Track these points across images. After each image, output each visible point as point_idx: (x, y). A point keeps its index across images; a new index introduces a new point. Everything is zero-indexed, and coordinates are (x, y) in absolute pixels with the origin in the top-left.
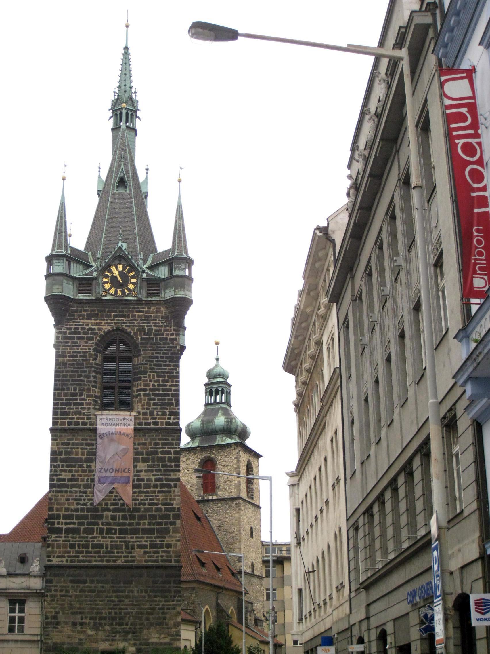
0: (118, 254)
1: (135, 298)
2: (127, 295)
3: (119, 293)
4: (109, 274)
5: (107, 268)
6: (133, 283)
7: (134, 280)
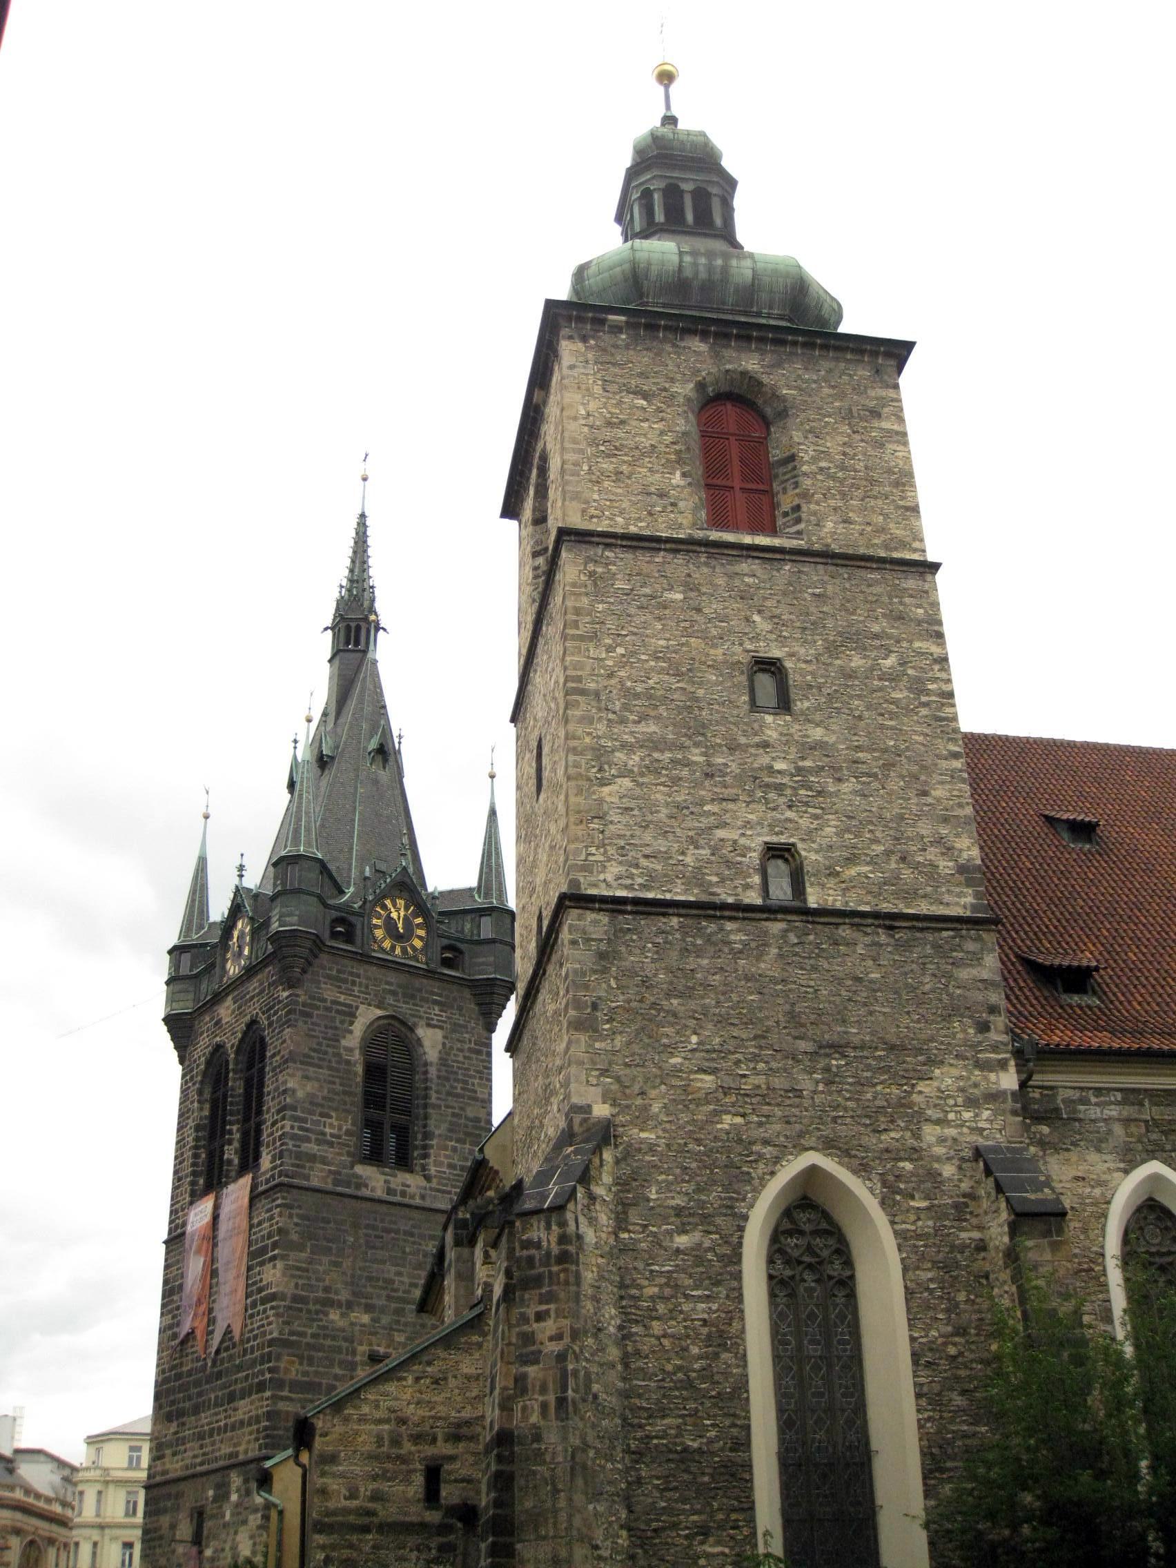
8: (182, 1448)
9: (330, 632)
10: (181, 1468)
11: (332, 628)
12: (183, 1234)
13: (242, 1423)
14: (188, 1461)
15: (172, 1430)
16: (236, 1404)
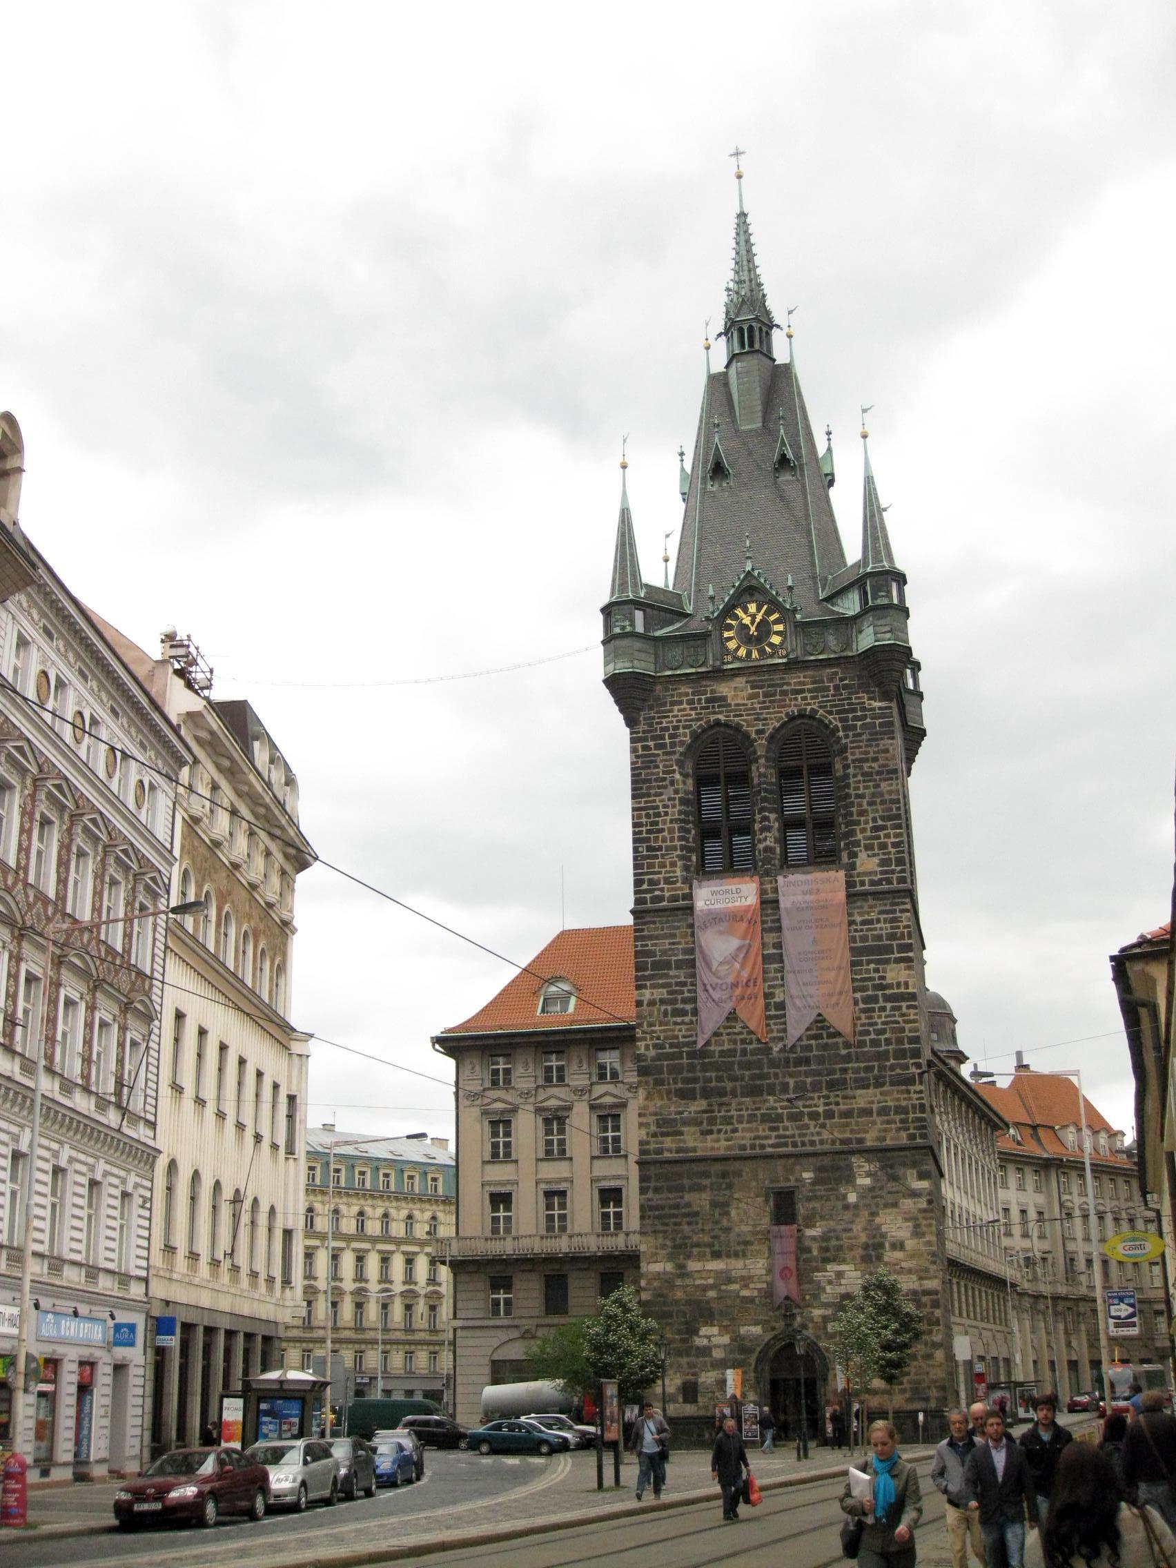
0: (746, 584)
1: (785, 660)
2: (772, 656)
3: (755, 654)
5: (728, 611)
6: (778, 633)
7: (780, 627)
8: (729, 1128)
9: (723, 337)
10: (728, 1148)
11: (726, 333)
12: (690, 909)
13: (867, 1112)
14: (748, 1143)
15: (693, 1109)
16: (849, 1092)
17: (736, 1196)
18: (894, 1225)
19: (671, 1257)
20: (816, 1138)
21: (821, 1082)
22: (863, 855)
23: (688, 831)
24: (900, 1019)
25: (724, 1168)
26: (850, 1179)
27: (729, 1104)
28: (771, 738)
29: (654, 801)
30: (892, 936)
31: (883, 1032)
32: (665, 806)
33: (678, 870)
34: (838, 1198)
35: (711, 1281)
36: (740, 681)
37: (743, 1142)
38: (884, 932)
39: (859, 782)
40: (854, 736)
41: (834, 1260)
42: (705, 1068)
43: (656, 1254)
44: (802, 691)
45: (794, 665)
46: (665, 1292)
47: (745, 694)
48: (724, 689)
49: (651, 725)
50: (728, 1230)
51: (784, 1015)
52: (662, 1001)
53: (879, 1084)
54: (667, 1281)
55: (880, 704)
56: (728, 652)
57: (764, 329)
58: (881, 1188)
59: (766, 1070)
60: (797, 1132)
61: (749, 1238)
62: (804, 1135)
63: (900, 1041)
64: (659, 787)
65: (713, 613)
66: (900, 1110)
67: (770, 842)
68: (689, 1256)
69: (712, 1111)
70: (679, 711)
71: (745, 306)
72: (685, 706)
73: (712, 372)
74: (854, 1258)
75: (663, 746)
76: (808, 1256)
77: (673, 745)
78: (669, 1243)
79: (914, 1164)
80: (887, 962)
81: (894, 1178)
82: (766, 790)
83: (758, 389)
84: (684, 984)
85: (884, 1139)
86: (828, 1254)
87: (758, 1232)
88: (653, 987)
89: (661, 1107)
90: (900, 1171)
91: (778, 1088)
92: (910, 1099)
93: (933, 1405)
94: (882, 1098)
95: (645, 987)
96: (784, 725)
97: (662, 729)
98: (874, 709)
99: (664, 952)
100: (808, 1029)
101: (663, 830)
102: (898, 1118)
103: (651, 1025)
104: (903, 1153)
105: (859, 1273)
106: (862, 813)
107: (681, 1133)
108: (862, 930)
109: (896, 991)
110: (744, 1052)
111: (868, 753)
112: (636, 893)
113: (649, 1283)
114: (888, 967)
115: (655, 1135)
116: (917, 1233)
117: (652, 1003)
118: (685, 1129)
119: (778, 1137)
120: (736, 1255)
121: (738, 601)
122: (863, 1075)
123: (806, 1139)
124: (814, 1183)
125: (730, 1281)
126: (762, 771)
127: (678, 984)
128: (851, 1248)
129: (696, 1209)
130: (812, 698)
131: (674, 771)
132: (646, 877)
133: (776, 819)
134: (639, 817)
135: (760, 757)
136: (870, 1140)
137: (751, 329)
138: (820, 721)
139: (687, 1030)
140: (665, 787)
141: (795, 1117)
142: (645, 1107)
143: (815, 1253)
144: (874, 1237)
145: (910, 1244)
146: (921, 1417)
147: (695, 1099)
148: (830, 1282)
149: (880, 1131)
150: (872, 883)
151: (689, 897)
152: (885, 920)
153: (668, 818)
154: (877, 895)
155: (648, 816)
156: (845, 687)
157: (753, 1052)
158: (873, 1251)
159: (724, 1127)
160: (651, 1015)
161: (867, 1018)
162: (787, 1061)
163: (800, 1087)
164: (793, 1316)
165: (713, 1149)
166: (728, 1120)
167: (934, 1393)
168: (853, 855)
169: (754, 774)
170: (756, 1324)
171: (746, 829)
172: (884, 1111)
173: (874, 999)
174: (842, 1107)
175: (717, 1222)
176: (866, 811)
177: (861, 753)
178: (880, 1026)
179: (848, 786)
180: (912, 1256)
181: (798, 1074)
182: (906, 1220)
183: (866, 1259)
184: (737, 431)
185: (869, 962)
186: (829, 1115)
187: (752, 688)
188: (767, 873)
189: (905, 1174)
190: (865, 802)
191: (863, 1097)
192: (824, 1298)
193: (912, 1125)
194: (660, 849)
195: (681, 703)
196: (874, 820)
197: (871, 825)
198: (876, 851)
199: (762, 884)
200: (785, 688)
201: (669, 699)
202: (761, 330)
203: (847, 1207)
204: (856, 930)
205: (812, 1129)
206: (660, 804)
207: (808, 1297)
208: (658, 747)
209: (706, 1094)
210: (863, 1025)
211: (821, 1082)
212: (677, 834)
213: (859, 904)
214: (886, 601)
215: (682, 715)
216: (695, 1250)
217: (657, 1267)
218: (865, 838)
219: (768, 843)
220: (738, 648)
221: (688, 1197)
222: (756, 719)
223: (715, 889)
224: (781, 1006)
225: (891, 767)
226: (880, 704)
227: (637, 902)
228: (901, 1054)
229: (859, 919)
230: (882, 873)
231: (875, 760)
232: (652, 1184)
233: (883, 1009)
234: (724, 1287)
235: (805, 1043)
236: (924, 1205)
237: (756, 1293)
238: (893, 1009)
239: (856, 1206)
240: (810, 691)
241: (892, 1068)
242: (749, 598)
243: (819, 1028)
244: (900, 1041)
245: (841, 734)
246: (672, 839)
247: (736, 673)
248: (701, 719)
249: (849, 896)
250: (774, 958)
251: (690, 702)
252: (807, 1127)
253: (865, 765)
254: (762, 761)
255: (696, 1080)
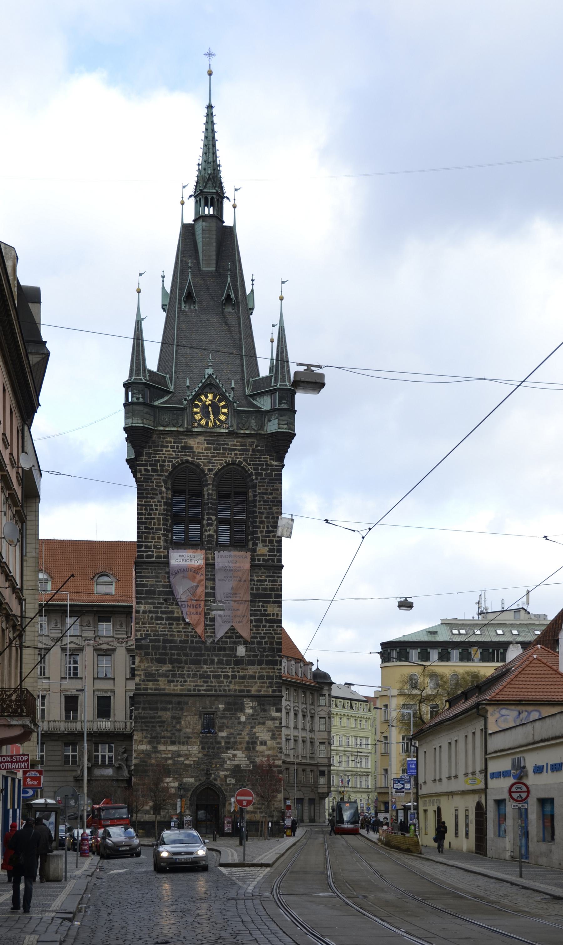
0: (208, 382)
1: (227, 431)
2: (219, 427)
4: (199, 403)
5: (197, 397)
6: (224, 414)
7: (225, 410)
8: (183, 680)
10: (181, 690)
12: (168, 563)
13: (253, 677)
14: (192, 688)
15: (164, 669)
16: (245, 667)
17: (184, 714)
18: (262, 733)
19: (150, 743)
20: (227, 688)
21: (231, 660)
22: (260, 545)
23: (167, 520)
24: (273, 632)
25: (179, 701)
26: (242, 710)
27: (183, 668)
28: (215, 475)
29: (150, 502)
30: (272, 590)
31: (264, 638)
32: (156, 505)
33: (162, 542)
34: (236, 719)
35: (170, 756)
36: (201, 439)
37: (189, 687)
38: (268, 587)
39: (261, 505)
40: (261, 479)
41: (232, 749)
42: (171, 648)
43: (142, 741)
44: (235, 450)
45: (231, 434)
46: (146, 760)
47: (203, 447)
48: (192, 442)
49: (150, 457)
50: (180, 731)
51: (214, 625)
52: (150, 612)
53: (260, 663)
54: (147, 754)
55: (276, 463)
56: (195, 421)
57: (220, 200)
58: (257, 715)
59: (203, 652)
60: (217, 684)
61: (190, 735)
62: (221, 686)
63: (272, 643)
64: (153, 494)
65: (188, 396)
66: (269, 677)
67: (211, 532)
68: (159, 743)
69: (175, 671)
70: (166, 451)
71: (210, 182)
72: (169, 449)
73: (186, 222)
74: (242, 748)
75: (156, 471)
76: (219, 745)
77: (162, 471)
78: (149, 736)
79: (274, 705)
80: (268, 602)
81: (264, 710)
82: (212, 503)
83: (214, 244)
84: (162, 604)
85: (261, 691)
86: (229, 745)
87: (195, 733)
88: (146, 603)
89: (148, 667)
90: (267, 707)
91: (209, 661)
92: (274, 672)
93: (275, 819)
94: (261, 671)
95: (141, 603)
96: (222, 468)
97: (156, 461)
98: (272, 466)
99: (152, 586)
100: (226, 633)
101: (154, 519)
102: (268, 681)
103: (143, 623)
104: (270, 699)
105: (244, 755)
106: (262, 522)
107: (158, 681)
108: (257, 585)
109: (272, 618)
110: (192, 642)
111: (267, 490)
112: (138, 552)
113: (138, 755)
114: (269, 605)
115: (144, 681)
116: (273, 738)
117: (145, 612)
118: (160, 679)
119: (207, 686)
120: (183, 743)
121: (203, 391)
122: (252, 658)
123: (222, 688)
124: (225, 710)
125: (179, 756)
126: (209, 492)
127: (159, 603)
128: (240, 743)
129: (163, 719)
130: (240, 455)
131: (161, 486)
132: (144, 544)
133: (216, 520)
134: (141, 509)
135: (209, 484)
136: (253, 690)
137: (212, 199)
138: (243, 467)
139: (163, 628)
140: (156, 494)
141: (217, 677)
142: (140, 666)
143: (223, 744)
144: (252, 738)
145: (269, 743)
146: (270, 825)
147: (165, 664)
148: (229, 759)
149: (259, 687)
150: (264, 560)
151: (167, 557)
152: (269, 580)
153: (157, 512)
154: (266, 567)
155: (146, 509)
156: (258, 451)
157: (197, 642)
158: (251, 746)
159: (180, 680)
160: (144, 619)
161: (256, 630)
162: (214, 648)
163: (220, 662)
164: (210, 774)
165: (174, 690)
166: (182, 676)
167: (276, 814)
168: (255, 544)
169: (205, 493)
170: (192, 777)
171: (199, 521)
172: (261, 677)
173: (260, 621)
174: (240, 674)
175: (175, 727)
176: (264, 521)
177: (264, 489)
178: (262, 635)
179: (255, 506)
180: (269, 749)
181: (220, 655)
182: (268, 731)
183: (248, 749)
184: (200, 270)
185: (259, 601)
186: (234, 677)
187: (208, 444)
188: (209, 549)
189: (269, 709)
190: (264, 516)
191: (252, 670)
192: (226, 766)
193: (275, 686)
194: (152, 529)
195: (167, 447)
196: (268, 527)
197: (266, 529)
198: (267, 544)
199: (206, 554)
200: (226, 446)
201: (160, 444)
202: (218, 200)
203: (240, 723)
204: (254, 584)
205: (225, 684)
206: (153, 504)
207: (218, 766)
208: (153, 471)
209: (171, 662)
210: (254, 633)
211: (231, 660)
212: (162, 522)
213: (256, 571)
214: (286, 406)
215: (167, 454)
216: (162, 740)
217: (142, 747)
218: (262, 536)
219: (211, 532)
220: (201, 419)
221: (160, 713)
222: (208, 462)
223: (182, 554)
224: (213, 620)
225: (279, 499)
226: (276, 463)
227: (140, 557)
228: (272, 650)
229: (256, 579)
230: (269, 555)
231: (271, 494)
232: (142, 706)
233: (265, 626)
234: (176, 759)
235: (224, 640)
236: (278, 725)
237: (192, 762)
238: (270, 627)
239: (244, 723)
240: (239, 450)
241: (267, 656)
242: (209, 391)
243: (231, 633)
244: (272, 643)
245: (254, 477)
246: (159, 524)
247: (199, 434)
248: (178, 458)
249: (252, 566)
250: (211, 595)
251: (173, 447)
252: (223, 682)
253: (266, 496)
254: (210, 486)
255: (166, 654)
